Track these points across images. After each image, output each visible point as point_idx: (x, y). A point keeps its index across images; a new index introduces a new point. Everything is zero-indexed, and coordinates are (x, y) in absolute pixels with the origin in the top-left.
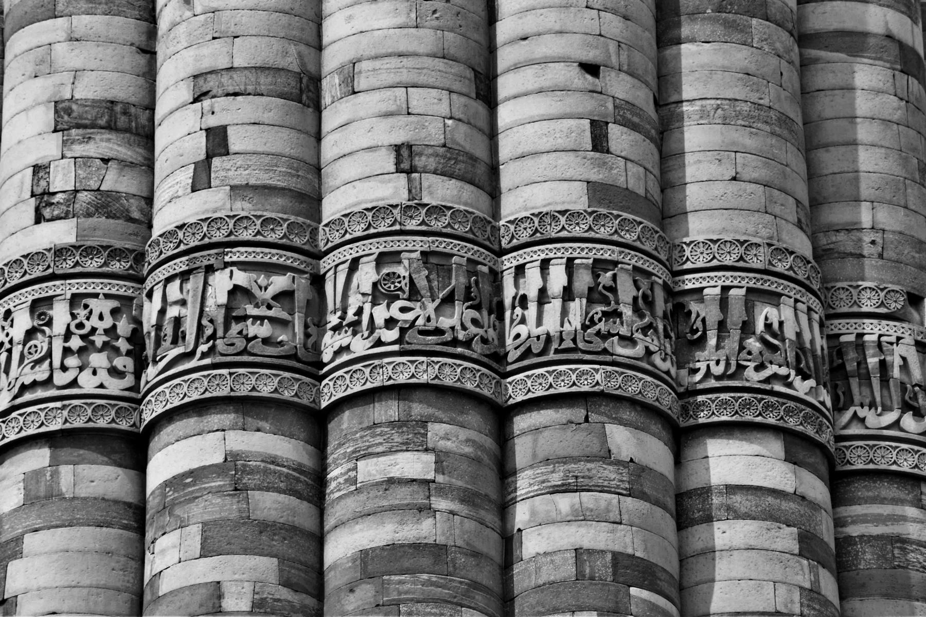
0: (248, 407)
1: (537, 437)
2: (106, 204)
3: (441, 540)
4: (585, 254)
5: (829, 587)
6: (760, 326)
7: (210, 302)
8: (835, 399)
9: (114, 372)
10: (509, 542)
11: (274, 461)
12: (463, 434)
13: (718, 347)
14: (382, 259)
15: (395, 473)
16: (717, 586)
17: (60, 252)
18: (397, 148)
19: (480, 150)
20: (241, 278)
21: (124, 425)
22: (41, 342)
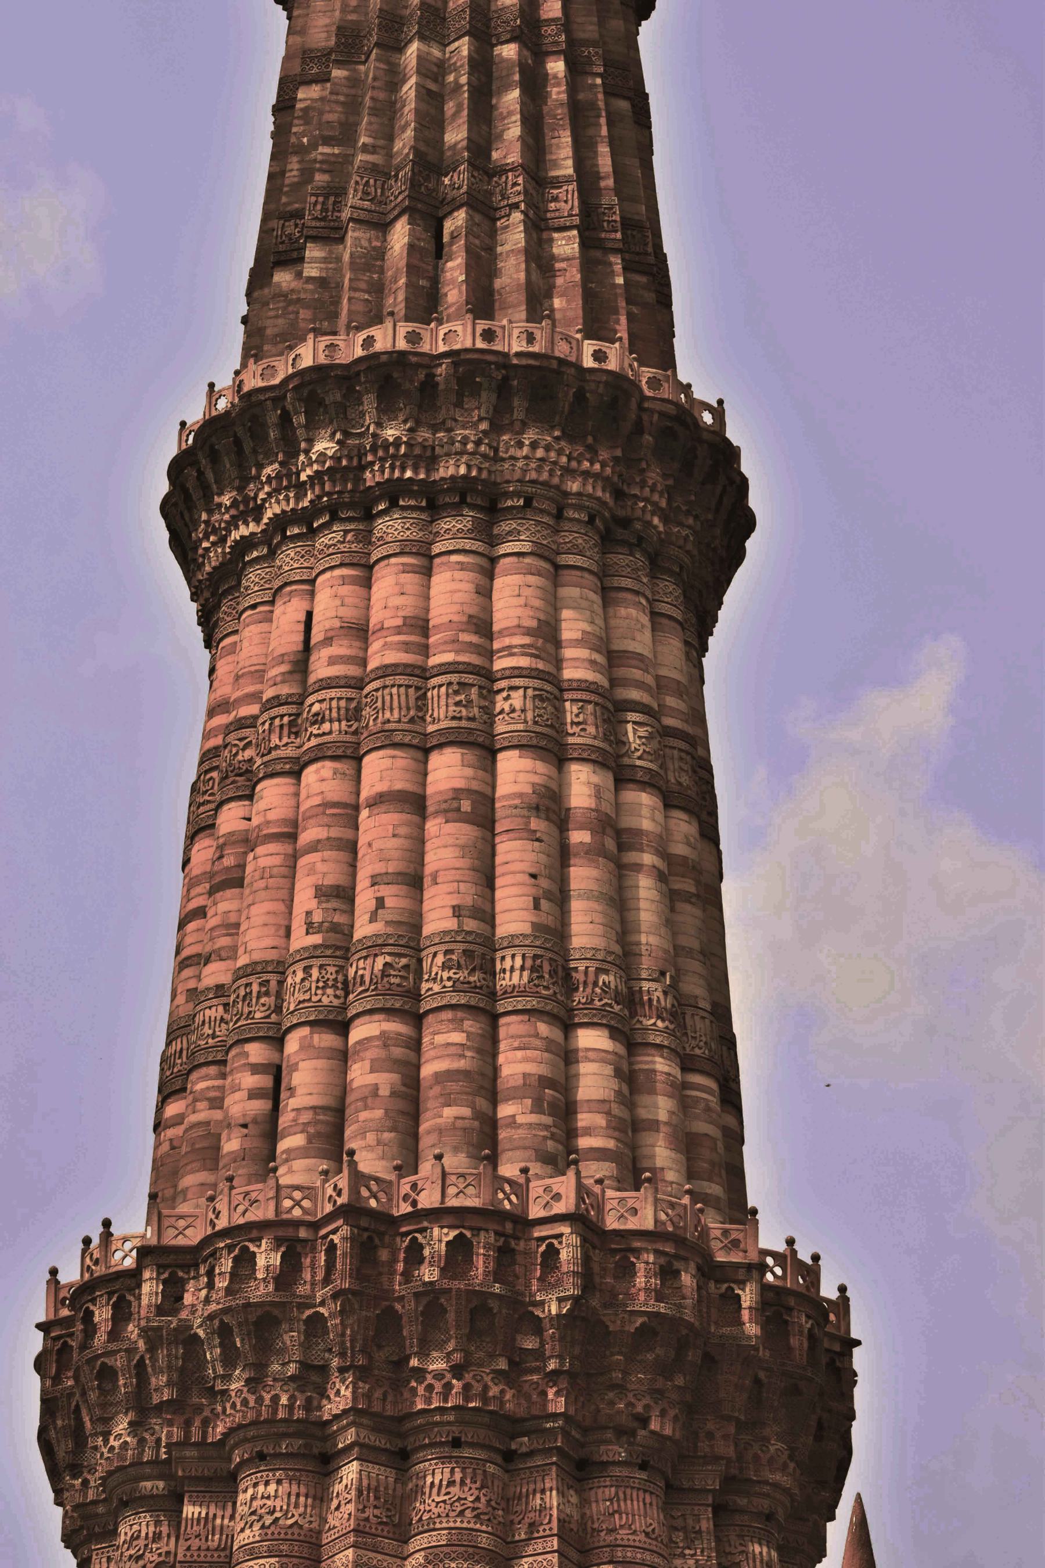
1: (510, 1027)
2: (335, 928)
3: (468, 1068)
4: (530, 952)
6: (601, 983)
7: (376, 969)
8: (630, 1013)
9: (336, 996)
10: (496, 1070)
11: (399, 1034)
12: (478, 1025)
13: (584, 991)
15: (450, 1041)
16: (580, 1089)
17: (315, 947)
18: (454, 907)
19: (488, 909)
20: (388, 959)
21: (340, 1018)
22: (307, 984)
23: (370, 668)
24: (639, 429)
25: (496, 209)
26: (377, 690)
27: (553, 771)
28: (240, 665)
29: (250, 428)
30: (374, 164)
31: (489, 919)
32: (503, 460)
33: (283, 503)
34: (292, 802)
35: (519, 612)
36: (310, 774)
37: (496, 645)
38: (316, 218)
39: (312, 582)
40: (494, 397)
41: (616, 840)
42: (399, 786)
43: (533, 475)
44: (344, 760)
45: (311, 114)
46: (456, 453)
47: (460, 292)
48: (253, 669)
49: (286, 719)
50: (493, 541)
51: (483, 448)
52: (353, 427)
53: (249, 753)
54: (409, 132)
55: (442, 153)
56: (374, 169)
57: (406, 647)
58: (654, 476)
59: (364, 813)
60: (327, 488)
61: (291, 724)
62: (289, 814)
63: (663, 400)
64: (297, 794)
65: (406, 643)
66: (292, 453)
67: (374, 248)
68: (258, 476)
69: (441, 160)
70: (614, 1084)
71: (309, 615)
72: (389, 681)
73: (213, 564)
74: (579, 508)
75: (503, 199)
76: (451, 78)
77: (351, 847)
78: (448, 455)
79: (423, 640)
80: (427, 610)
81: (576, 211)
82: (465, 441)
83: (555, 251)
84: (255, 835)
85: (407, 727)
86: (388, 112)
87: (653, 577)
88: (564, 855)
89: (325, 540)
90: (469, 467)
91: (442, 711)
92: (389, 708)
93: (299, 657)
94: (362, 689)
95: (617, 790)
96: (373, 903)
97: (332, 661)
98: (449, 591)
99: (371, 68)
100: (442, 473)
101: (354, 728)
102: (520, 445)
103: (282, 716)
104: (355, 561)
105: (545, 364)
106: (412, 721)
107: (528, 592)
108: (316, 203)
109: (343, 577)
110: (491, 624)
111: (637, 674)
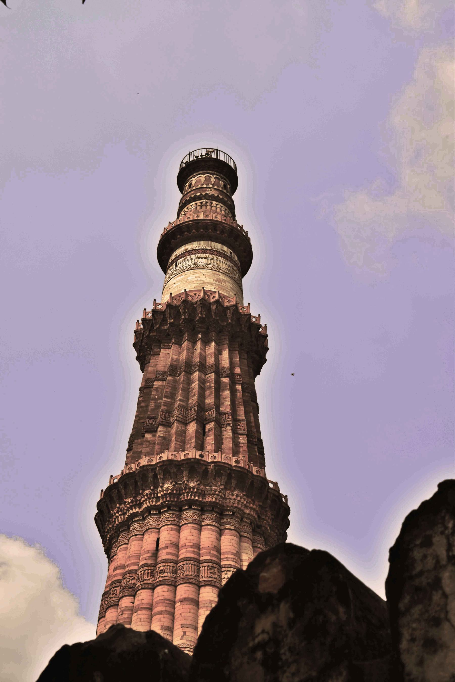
23: (179, 558)
24: (267, 498)
25: (222, 425)
26: (184, 565)
28: (130, 554)
29: (142, 478)
30: (183, 405)
33: (151, 503)
34: (151, 598)
35: (230, 547)
37: (222, 557)
38: (162, 419)
39: (159, 529)
40: (226, 478)
42: (191, 596)
43: (237, 505)
46: (213, 494)
48: (135, 555)
49: (150, 571)
50: (221, 524)
51: (221, 494)
52: (178, 481)
53: (133, 582)
54: (195, 397)
55: (205, 405)
56: (183, 407)
57: (194, 552)
58: (269, 514)
59: (178, 604)
60: (168, 499)
62: (150, 602)
64: (152, 596)
65: (194, 551)
68: (142, 494)
69: (204, 407)
72: (188, 562)
73: (119, 521)
74: (248, 518)
75: (224, 422)
76: (208, 384)
77: (173, 615)
78: (209, 494)
79: (199, 552)
80: (200, 542)
81: (246, 430)
82: (215, 491)
83: (240, 440)
84: (137, 607)
85: (194, 578)
86: (187, 392)
87: (265, 545)
90: (216, 499)
91: (205, 574)
92: (188, 570)
93: (154, 552)
94: (177, 564)
96: (182, 634)
97: (168, 554)
98: (207, 537)
99: (182, 377)
100: (207, 500)
103: (148, 570)
106: (195, 576)
107: (232, 541)
108: (162, 414)
109: (171, 528)
110: (220, 550)
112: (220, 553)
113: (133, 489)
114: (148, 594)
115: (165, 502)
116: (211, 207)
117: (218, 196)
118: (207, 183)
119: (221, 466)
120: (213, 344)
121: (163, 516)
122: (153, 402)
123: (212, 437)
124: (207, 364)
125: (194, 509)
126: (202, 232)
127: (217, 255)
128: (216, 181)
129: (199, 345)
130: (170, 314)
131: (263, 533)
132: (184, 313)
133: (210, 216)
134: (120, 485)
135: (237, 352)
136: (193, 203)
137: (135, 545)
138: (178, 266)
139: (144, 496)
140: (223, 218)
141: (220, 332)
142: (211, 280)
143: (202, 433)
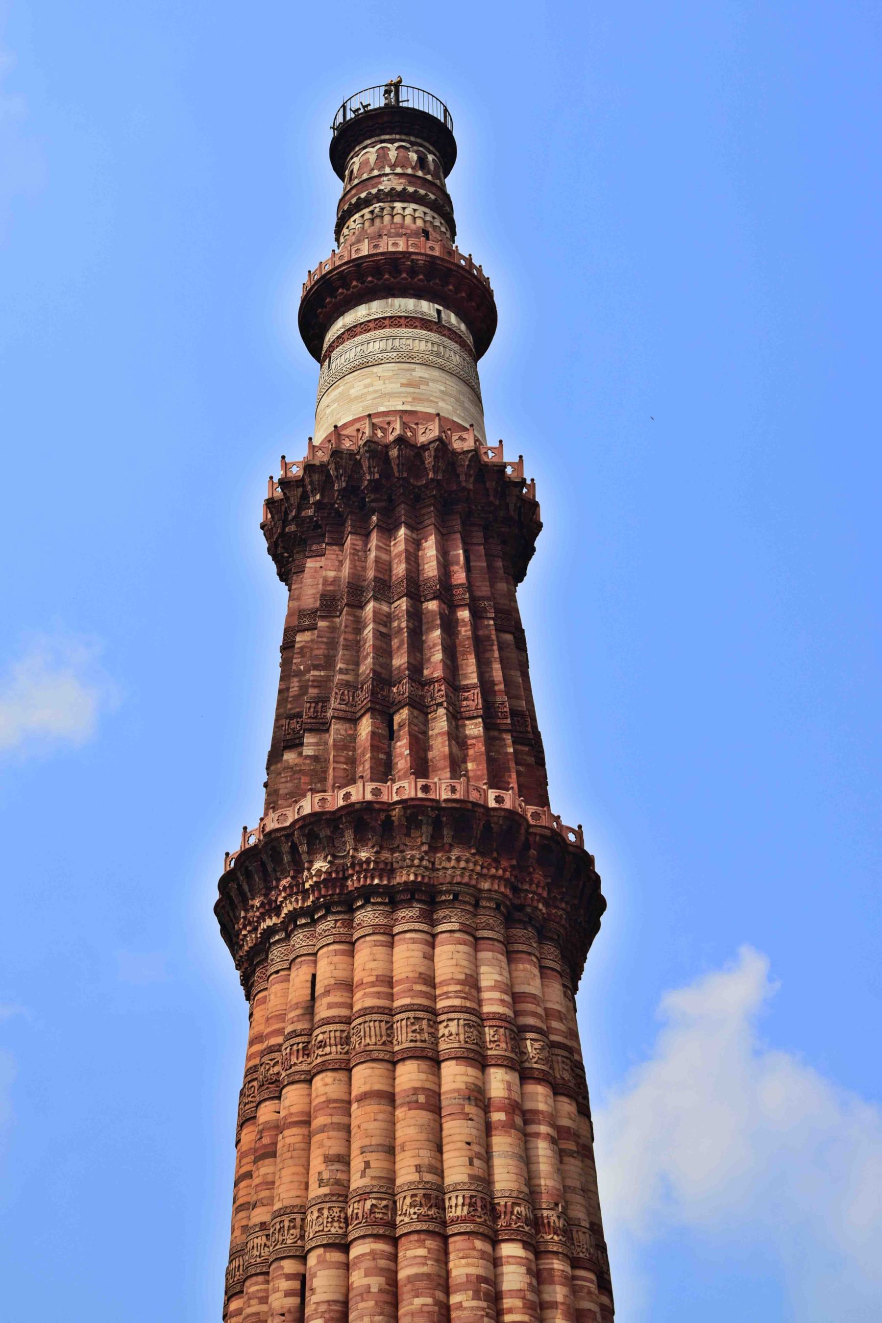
0: (376, 1237)
1: (456, 1244)
2: (338, 1182)
4: (468, 1194)
5: (535, 1282)
6: (515, 1212)
9: (340, 1228)
10: (448, 1272)
11: (383, 1251)
14: (412, 1196)
15: (417, 1254)
17: (325, 1195)
18: (416, 1166)
20: (374, 1202)
21: (343, 1242)
22: (320, 1220)
23: (355, 1010)
24: (527, 846)
26: (360, 1024)
27: (478, 1073)
30: (347, 681)
31: (441, 1174)
32: (438, 870)
33: (294, 903)
34: (307, 1100)
35: (452, 969)
36: (318, 1081)
37: (438, 992)
39: (315, 954)
40: (431, 828)
41: (522, 1117)
42: (377, 1087)
43: (458, 879)
44: (340, 1071)
45: (306, 650)
46: (407, 867)
47: (406, 761)
48: (277, 1013)
49: (301, 1046)
50: (433, 923)
51: (424, 863)
52: (339, 852)
53: (276, 1069)
55: (391, 672)
56: (347, 684)
57: (378, 995)
58: (538, 876)
59: (355, 1106)
60: (323, 893)
61: (304, 1048)
62: (306, 1109)
63: (541, 827)
64: (310, 1095)
66: (299, 871)
67: (349, 735)
68: (277, 887)
69: (391, 677)
70: (527, 1279)
71: (314, 976)
72: (368, 1018)
73: (250, 945)
74: (489, 899)
76: (395, 624)
77: (348, 1129)
78: (402, 868)
79: (389, 990)
81: (480, 706)
82: (412, 859)
83: (467, 732)
86: (355, 646)
87: (540, 942)
88: (488, 1129)
89: (323, 927)
90: (416, 875)
91: (403, 1038)
92: (368, 1035)
93: (308, 1004)
94: (350, 1024)
95: (521, 1084)
96: (363, 1165)
97: (330, 1006)
98: (406, 957)
99: (343, 620)
101: (346, 1050)
102: (449, 859)
103: (298, 1044)
104: (343, 940)
105: (464, 806)
106: (384, 1044)
107: (456, 956)
111: (530, 1007)
112: (434, 986)
113: (260, 880)
114: (297, 1093)
115: (318, 899)
116: (393, 216)
117: (404, 189)
118: (381, 164)
119: (414, 806)
120: (402, 531)
121: (321, 927)
122: (296, 679)
123: (405, 741)
124: (394, 578)
125: (374, 904)
126: (371, 282)
127: (406, 326)
128: (401, 154)
129: (374, 540)
130: (311, 483)
131: (531, 919)
132: (337, 477)
133: (381, 245)
134: (239, 874)
135: (458, 536)
136: (357, 216)
137: (276, 994)
138: (333, 366)
139: (280, 891)
140: (410, 243)
141: (416, 500)
142: (395, 387)
143: (385, 737)
